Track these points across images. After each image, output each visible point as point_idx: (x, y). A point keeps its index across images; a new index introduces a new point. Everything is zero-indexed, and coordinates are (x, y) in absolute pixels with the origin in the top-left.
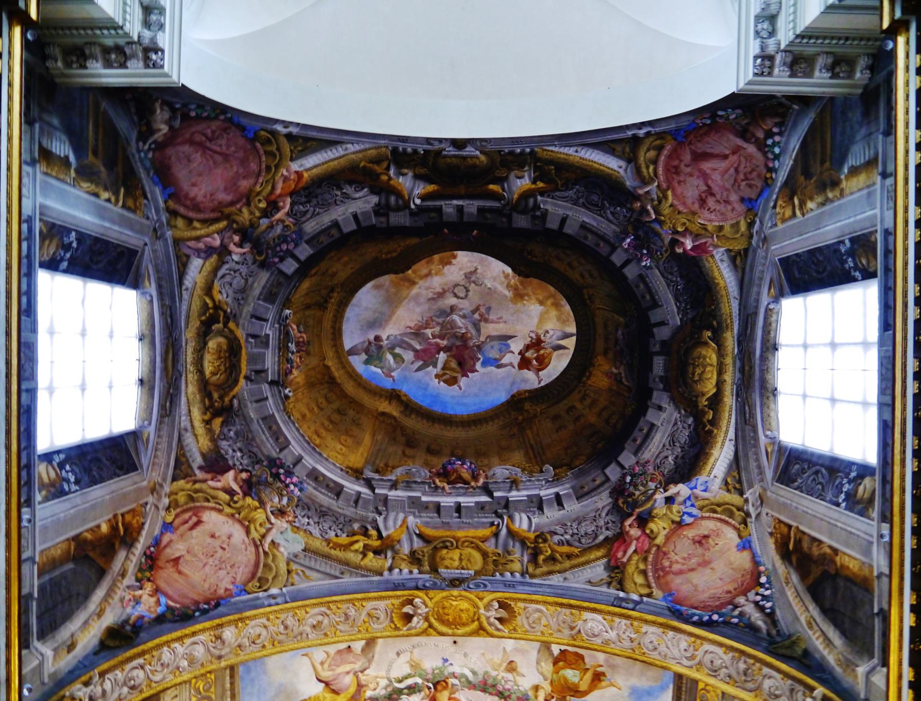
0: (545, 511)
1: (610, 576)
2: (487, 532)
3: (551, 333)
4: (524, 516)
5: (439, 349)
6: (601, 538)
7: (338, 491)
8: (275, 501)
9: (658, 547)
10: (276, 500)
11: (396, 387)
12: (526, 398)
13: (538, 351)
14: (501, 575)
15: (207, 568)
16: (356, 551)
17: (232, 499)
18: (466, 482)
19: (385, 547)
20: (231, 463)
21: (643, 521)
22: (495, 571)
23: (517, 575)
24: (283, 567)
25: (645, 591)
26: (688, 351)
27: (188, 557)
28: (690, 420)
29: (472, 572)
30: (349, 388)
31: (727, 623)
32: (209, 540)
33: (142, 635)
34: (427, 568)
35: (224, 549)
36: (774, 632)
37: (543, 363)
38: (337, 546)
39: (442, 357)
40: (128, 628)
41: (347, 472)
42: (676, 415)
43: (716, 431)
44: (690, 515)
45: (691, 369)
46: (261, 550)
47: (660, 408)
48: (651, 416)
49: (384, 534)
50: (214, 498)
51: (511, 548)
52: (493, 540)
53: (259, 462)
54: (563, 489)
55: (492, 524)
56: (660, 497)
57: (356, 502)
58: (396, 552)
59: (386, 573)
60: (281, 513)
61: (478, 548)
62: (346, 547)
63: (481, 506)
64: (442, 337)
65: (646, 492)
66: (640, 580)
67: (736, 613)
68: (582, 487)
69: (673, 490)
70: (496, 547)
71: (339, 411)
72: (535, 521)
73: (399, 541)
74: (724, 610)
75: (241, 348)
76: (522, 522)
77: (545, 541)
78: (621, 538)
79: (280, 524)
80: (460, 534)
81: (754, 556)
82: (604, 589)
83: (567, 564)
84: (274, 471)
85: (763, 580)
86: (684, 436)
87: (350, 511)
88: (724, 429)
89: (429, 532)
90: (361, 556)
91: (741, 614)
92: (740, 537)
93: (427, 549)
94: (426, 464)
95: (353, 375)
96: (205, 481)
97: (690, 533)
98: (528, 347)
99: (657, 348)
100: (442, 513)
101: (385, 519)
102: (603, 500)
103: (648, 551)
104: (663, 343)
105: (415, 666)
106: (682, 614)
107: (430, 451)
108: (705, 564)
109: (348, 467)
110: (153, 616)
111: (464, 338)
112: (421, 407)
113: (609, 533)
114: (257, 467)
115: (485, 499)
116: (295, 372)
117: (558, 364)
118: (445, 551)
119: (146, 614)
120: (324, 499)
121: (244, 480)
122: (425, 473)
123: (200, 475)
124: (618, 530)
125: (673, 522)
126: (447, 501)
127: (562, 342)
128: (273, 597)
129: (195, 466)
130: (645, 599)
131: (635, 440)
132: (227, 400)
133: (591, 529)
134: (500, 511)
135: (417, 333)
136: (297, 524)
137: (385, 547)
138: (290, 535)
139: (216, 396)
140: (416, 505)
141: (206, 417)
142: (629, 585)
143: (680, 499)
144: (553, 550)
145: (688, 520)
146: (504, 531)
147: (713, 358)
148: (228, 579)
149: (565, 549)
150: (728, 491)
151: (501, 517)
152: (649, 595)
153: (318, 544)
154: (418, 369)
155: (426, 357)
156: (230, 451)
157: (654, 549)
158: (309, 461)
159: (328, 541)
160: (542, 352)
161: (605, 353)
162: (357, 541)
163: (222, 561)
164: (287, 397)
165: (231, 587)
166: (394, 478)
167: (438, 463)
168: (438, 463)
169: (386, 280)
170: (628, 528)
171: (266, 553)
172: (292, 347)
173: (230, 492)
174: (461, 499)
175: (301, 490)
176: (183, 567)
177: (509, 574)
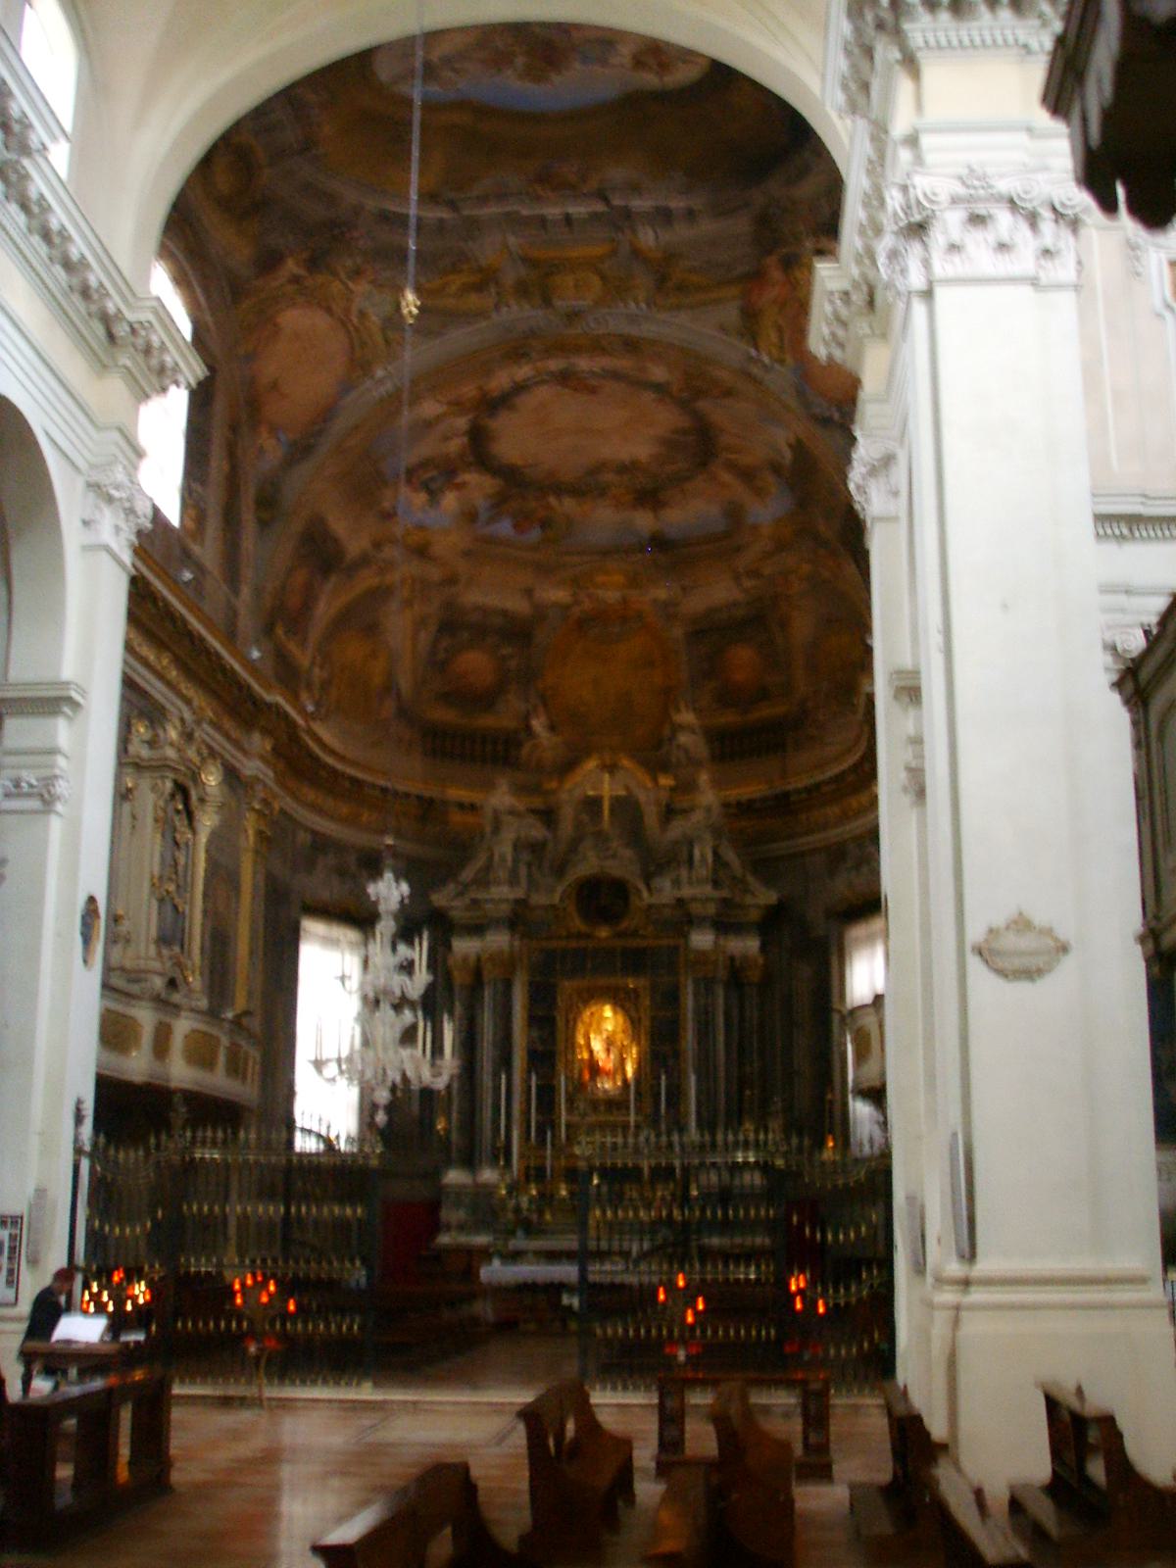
4: (650, 233)
19: (485, 280)
23: (643, 305)
24: (379, 338)
37: (663, 67)
46: (351, 329)
54: (697, 202)
59: (494, 315)
60: (357, 273)
63: (595, 217)
66: (773, 337)
76: (647, 238)
79: (361, 287)
80: (574, 253)
102: (741, 225)
115: (600, 207)
126: (553, 212)
128: (381, 381)
130: (777, 366)
137: (485, 280)
140: (514, 221)
152: (782, 362)
158: (372, 204)
173: (295, 280)
177: (632, 305)
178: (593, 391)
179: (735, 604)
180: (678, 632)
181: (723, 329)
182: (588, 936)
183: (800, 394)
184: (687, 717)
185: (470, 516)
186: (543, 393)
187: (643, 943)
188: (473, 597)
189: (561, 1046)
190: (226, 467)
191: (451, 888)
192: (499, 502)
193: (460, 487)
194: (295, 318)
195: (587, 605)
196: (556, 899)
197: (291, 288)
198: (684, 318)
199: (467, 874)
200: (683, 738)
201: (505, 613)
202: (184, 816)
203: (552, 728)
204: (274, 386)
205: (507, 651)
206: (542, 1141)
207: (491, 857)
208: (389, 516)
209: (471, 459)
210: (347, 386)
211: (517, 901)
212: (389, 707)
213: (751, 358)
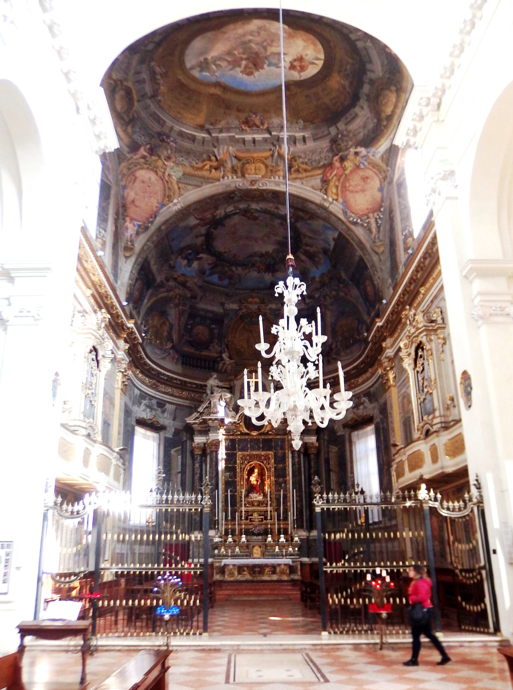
0: (297, 145)
1: (323, 187)
2: (268, 154)
3: (309, 56)
5: (242, 59)
6: (322, 164)
7: (193, 139)
8: (165, 153)
9: (346, 175)
10: (165, 153)
11: (219, 80)
12: (292, 85)
13: (301, 62)
14: (274, 178)
15: (146, 199)
16: (207, 170)
17: (146, 160)
18: (258, 127)
19: (220, 165)
20: (140, 143)
21: (342, 159)
22: (271, 175)
23: (281, 178)
24: (176, 187)
25: (335, 197)
26: (382, 89)
27: (137, 197)
28: (375, 120)
29: (260, 176)
30: (193, 86)
31: (362, 225)
32: (142, 185)
33: (136, 245)
34: (240, 175)
35: (149, 186)
36: (377, 236)
37: (303, 69)
38: (198, 169)
39: (244, 63)
40: (129, 243)
41: (197, 128)
42: (369, 115)
43: (385, 131)
44: (363, 164)
45: (382, 98)
47: (362, 108)
48: (357, 109)
49: (218, 158)
50: (138, 163)
51: (279, 163)
52: (271, 158)
53: (153, 137)
54: (307, 134)
55: (271, 150)
56: (352, 150)
57: (203, 143)
58: (225, 167)
59: (221, 180)
60: (169, 158)
61: (263, 163)
62: (201, 169)
63: (265, 140)
64: (244, 53)
65: (346, 146)
66: (334, 191)
67: (367, 221)
68: (317, 135)
69: (359, 149)
70: (272, 162)
71: (188, 98)
72: (291, 149)
73: (226, 161)
74: (363, 218)
75: (131, 89)
77: (295, 161)
78: (330, 165)
79: (170, 164)
80: (255, 155)
81: (382, 197)
82: (318, 192)
83: (305, 174)
84: (161, 138)
85: (382, 209)
86: (371, 126)
87: (200, 149)
88: (389, 132)
89: (240, 155)
90: (209, 172)
91: (369, 223)
92: (381, 184)
93: (239, 164)
94: (238, 118)
95: (194, 79)
96: (131, 158)
97: (361, 173)
98: (295, 60)
99: (367, 81)
100: (246, 144)
101: (218, 150)
102: (325, 144)
103: (341, 176)
104: (371, 80)
105: (236, 208)
106: (347, 214)
107: (239, 110)
108: (363, 190)
109: (197, 125)
110: (135, 233)
111: (257, 54)
112: (232, 88)
113: (326, 162)
114: (153, 140)
115: (267, 136)
116: (162, 88)
117: (312, 71)
118: (248, 165)
119: (132, 233)
120: (187, 145)
121: (149, 149)
122: (236, 123)
123: (129, 156)
124: (330, 161)
125: (355, 165)
126: (248, 137)
127: (315, 62)
128: (175, 204)
129: (125, 153)
131: (347, 118)
132: (131, 116)
133: (318, 158)
134: (275, 143)
135: (229, 53)
136: (177, 162)
137: (220, 165)
138: (175, 168)
139: (125, 117)
141: (124, 129)
142: (329, 193)
143: (362, 155)
144: (299, 166)
145: (362, 166)
146: (276, 154)
147: (394, 100)
148: (155, 201)
149: (304, 166)
150: (382, 161)
151: (275, 147)
152: (337, 200)
153: (189, 170)
154: (231, 69)
155: (235, 63)
156: (139, 138)
157: (344, 176)
158: (177, 128)
159: (193, 167)
160: (303, 64)
161: (339, 72)
162: (206, 165)
163: (150, 193)
164: (160, 101)
165: (158, 205)
166: (220, 127)
167: (243, 116)
168: (243, 116)
169: (209, 34)
170: (335, 161)
171: (167, 181)
172: (158, 77)
173: (144, 157)
174: (255, 136)
175: (176, 143)
176: (137, 203)
177: (277, 177)
178: (256, 219)
181: (313, 187)
183: (345, 213)
185: (202, 272)
186: (236, 219)
187: (270, 437)
188: (202, 305)
190: (114, 228)
191: (195, 415)
192: (214, 266)
193: (200, 259)
194: (143, 174)
195: (244, 311)
196: (236, 421)
197: (142, 160)
198: (298, 183)
199: (201, 409)
201: (212, 312)
202: (96, 362)
203: (230, 358)
204: (133, 201)
205: (214, 326)
207: (210, 403)
208: (172, 268)
209: (204, 247)
210: (163, 205)
212: (169, 345)
213: (324, 199)
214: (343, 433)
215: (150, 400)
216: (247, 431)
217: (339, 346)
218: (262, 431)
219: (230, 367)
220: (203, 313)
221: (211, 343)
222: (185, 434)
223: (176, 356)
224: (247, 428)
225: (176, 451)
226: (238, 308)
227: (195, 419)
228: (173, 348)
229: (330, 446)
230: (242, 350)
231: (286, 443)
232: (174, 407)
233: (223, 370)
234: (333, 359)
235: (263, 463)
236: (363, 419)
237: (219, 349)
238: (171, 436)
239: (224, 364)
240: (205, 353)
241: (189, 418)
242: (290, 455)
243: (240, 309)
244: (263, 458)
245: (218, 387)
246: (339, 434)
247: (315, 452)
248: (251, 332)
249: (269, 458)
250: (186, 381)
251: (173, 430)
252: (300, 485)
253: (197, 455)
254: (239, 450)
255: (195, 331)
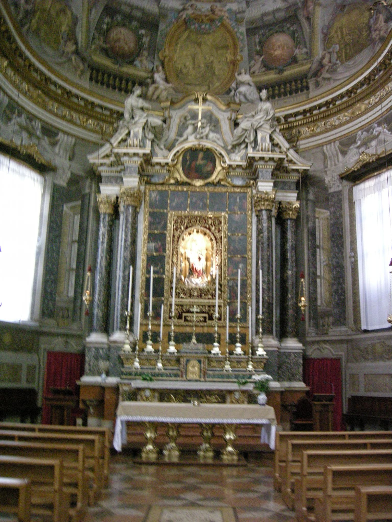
179: (279, 10)
180: (243, 29)
182: (188, 184)
184: (246, 78)
187: (224, 190)
189: (168, 253)
195: (190, 12)
196: (169, 160)
200: (243, 89)
201: (142, 10)
203: (166, 80)
205: (142, 32)
206: (157, 316)
207: (129, 134)
211: (144, 155)
212: (71, 48)
214: (338, 189)
215: (31, 120)
216: (185, 179)
217: (334, 60)
218: (210, 180)
219: (165, 94)
220: (127, 10)
221: (138, 55)
222: (88, 182)
223: (81, 66)
224: (187, 174)
225: (72, 208)
226: (181, 7)
227: (104, 157)
228: (76, 52)
229: (317, 209)
230: (185, 71)
231: (249, 200)
232: (71, 140)
233: (155, 97)
234: (324, 79)
235: (209, 229)
236: (378, 159)
237: (150, 66)
238: (65, 184)
239: (157, 88)
240: (127, 69)
241: (95, 155)
242: (255, 219)
243: (184, 9)
244: (210, 222)
245: (142, 109)
246: (331, 190)
247: (294, 217)
248: (199, 45)
249: (220, 223)
250: (93, 103)
251: (69, 175)
252: (270, 264)
253: (105, 214)
254: (173, 209)
255: (113, 35)
